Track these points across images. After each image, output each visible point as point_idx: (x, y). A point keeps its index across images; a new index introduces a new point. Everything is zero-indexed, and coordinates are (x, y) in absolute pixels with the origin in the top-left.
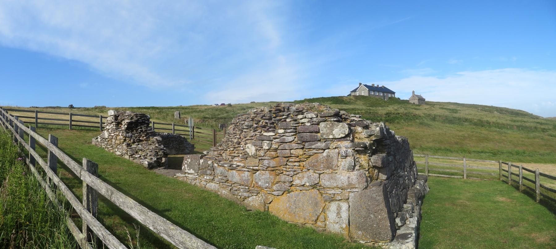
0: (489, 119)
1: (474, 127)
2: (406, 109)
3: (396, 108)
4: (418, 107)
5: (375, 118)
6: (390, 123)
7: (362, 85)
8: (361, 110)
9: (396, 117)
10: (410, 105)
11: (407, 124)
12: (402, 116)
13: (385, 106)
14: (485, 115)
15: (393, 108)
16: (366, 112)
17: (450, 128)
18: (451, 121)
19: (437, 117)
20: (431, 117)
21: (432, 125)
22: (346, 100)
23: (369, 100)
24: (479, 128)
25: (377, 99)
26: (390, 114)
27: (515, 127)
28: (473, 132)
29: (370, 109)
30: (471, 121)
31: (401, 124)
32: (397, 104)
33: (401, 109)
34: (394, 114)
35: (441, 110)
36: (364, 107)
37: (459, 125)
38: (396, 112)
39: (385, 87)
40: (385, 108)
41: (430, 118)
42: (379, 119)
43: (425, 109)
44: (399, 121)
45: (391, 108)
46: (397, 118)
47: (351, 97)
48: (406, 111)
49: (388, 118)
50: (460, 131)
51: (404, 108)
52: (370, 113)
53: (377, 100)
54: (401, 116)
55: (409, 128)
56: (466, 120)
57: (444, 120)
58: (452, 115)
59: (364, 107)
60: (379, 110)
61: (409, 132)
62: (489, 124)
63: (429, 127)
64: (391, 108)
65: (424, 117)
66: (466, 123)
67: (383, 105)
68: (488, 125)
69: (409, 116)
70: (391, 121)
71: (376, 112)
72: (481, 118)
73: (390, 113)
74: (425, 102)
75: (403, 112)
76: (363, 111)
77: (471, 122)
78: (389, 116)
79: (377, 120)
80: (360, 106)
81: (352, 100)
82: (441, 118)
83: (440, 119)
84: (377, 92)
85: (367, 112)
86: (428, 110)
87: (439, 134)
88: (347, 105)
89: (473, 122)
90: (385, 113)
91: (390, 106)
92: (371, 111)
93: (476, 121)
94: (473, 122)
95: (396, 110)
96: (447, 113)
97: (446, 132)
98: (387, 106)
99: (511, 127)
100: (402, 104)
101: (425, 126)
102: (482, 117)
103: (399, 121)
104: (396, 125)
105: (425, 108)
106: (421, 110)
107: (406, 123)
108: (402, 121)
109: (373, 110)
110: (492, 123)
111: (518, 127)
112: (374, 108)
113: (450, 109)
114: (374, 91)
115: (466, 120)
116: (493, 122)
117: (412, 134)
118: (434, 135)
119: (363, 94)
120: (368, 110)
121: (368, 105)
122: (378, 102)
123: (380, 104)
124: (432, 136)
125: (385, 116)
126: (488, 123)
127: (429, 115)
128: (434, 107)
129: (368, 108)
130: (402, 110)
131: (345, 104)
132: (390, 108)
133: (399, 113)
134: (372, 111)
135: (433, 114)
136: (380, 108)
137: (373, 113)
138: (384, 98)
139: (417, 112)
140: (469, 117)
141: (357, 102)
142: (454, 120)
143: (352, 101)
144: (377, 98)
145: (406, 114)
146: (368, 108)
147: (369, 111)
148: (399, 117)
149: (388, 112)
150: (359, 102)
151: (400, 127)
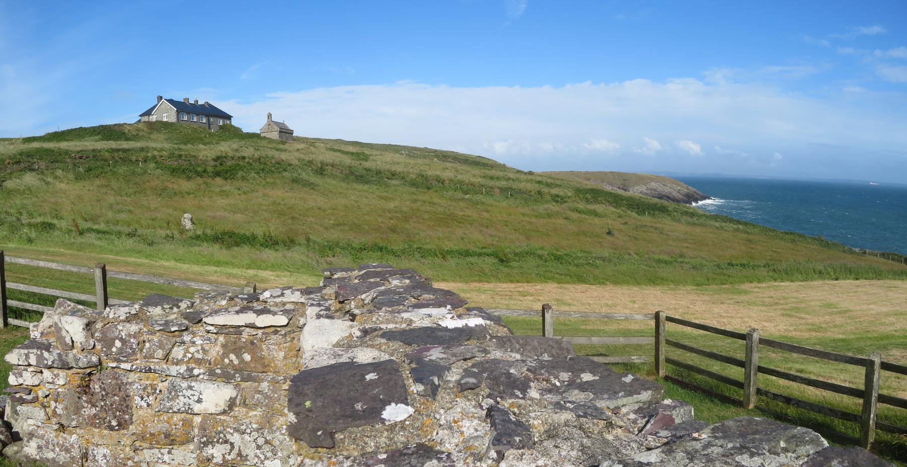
0: (438, 173)
1: (414, 189)
2: (258, 150)
3: (235, 146)
4: (281, 146)
5: (191, 168)
7: (163, 100)
8: (162, 150)
9: (239, 165)
10: (264, 143)
11: (263, 182)
12: (251, 164)
16: (171, 156)
17: (362, 193)
18: (362, 176)
22: (129, 130)
23: (178, 131)
24: (424, 192)
26: (225, 160)
27: (497, 191)
28: (416, 201)
30: (403, 178)
31: (250, 181)
33: (247, 148)
34: (233, 158)
35: (331, 153)
36: (167, 145)
38: (238, 154)
40: (212, 146)
42: (199, 169)
43: (298, 150)
45: (226, 147)
46: (241, 168)
47: (140, 126)
48: (257, 154)
49: (220, 168)
51: (252, 146)
52: (180, 156)
53: (195, 130)
54: (248, 163)
56: (393, 175)
57: (346, 175)
59: (167, 145)
62: (442, 183)
63: (313, 189)
64: (226, 147)
66: (394, 182)
67: (207, 140)
69: (265, 164)
70: (228, 175)
71: (194, 154)
72: (421, 170)
73: (225, 157)
74: (292, 137)
75: (254, 155)
76: (164, 153)
77: (404, 180)
78: (221, 164)
80: (159, 144)
81: (143, 130)
84: (194, 115)
85: (174, 154)
86: (304, 151)
89: (408, 179)
90: (213, 157)
91: (223, 143)
93: (414, 177)
94: (408, 179)
95: (237, 150)
96: (348, 160)
97: (357, 202)
98: (217, 143)
99: (490, 191)
100: (247, 140)
101: (304, 185)
102: (422, 168)
105: (296, 149)
108: (253, 174)
110: (448, 182)
111: (502, 190)
112: (189, 146)
113: (353, 154)
114: (188, 113)
115: (394, 175)
116: (451, 180)
117: (279, 204)
119: (165, 120)
120: (176, 150)
121: (175, 141)
122: (197, 135)
125: (213, 163)
127: (309, 162)
128: (314, 147)
129: (176, 146)
130: (249, 152)
131: (127, 139)
132: (223, 146)
133: (244, 158)
134: (183, 153)
136: (202, 146)
137: (186, 157)
139: (284, 156)
141: (152, 136)
142: (368, 175)
143: (141, 133)
145: (259, 159)
146: (176, 146)
147: (176, 152)
148: (245, 166)
149: (219, 154)
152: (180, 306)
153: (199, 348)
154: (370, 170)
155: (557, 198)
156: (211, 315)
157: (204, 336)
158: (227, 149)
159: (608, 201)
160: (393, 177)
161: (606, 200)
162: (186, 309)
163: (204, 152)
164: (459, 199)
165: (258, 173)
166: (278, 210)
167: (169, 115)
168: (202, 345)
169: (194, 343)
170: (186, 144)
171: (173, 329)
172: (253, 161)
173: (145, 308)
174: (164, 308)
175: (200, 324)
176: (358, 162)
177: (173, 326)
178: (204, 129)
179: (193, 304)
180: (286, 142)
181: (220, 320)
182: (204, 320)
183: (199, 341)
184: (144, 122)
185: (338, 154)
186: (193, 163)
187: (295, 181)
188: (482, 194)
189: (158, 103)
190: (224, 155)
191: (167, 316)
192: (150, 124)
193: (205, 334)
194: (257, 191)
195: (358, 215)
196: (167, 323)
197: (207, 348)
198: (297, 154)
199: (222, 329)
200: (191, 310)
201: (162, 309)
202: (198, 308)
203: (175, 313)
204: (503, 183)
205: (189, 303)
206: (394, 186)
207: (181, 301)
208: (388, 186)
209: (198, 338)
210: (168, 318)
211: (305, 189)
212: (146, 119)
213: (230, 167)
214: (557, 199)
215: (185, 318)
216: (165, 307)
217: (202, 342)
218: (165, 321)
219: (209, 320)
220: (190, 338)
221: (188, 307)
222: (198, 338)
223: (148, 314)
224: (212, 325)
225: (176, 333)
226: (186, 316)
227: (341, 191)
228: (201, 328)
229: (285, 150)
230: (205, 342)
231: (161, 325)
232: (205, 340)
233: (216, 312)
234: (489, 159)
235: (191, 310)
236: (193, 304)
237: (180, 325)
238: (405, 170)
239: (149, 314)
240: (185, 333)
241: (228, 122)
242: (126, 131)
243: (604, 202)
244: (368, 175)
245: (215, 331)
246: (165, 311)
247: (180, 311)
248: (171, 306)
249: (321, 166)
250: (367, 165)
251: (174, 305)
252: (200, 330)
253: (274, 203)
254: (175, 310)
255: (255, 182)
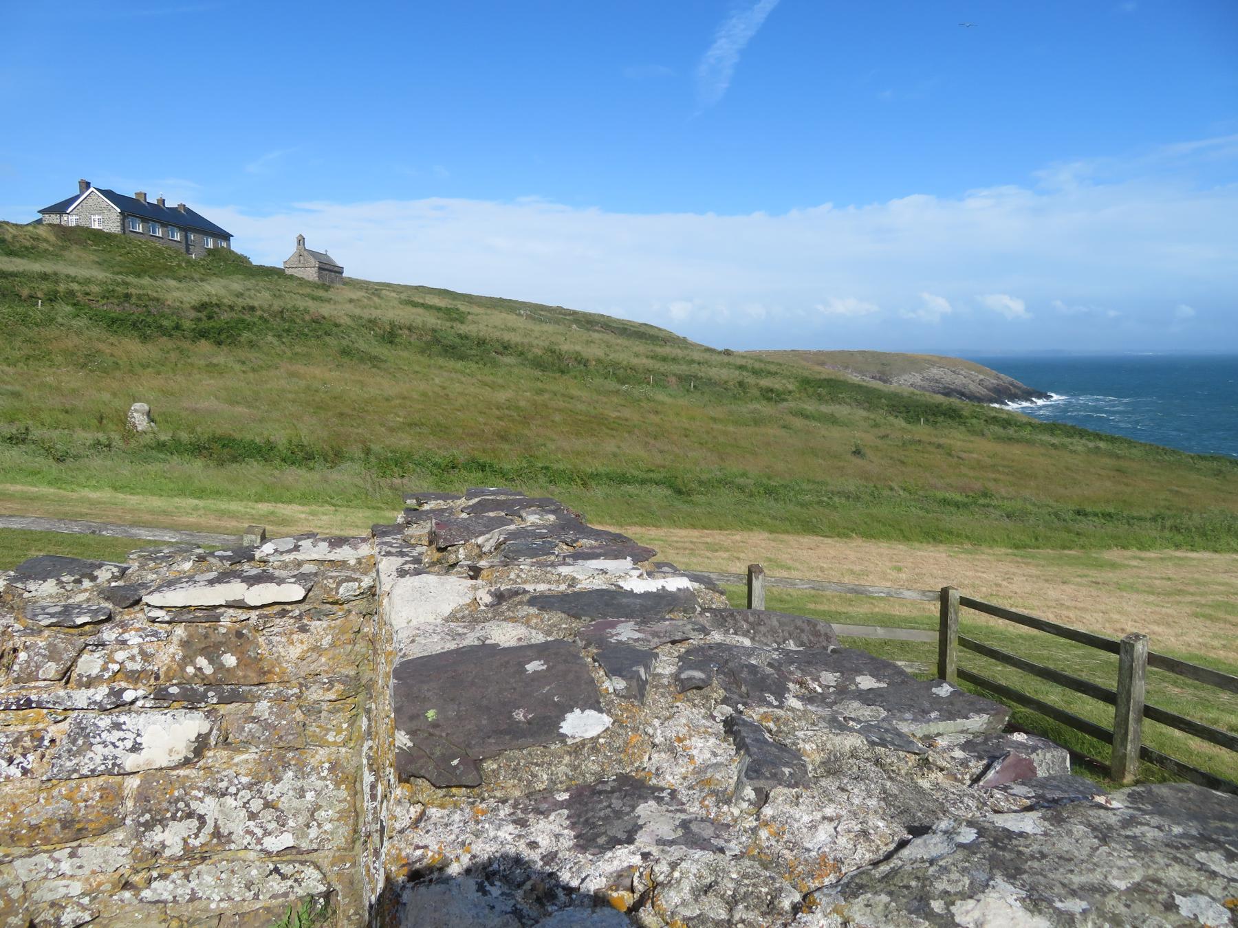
0: (578, 348)
1: (538, 373)
2: (280, 296)
4: (321, 293)
5: (149, 320)
6: (219, 343)
7: (92, 189)
8: (88, 281)
9: (243, 321)
10: (292, 285)
12: (266, 321)
13: (192, 279)
14: (562, 334)
15: (224, 287)
16: (108, 295)
17: (453, 375)
19: (400, 332)
20: (376, 329)
21: (386, 361)
22: (14, 237)
23: (124, 251)
25: (160, 251)
26: (216, 310)
27: (673, 380)
28: (540, 392)
29: (126, 284)
30: (522, 353)
32: (240, 277)
34: (231, 308)
35: (410, 309)
36: (101, 275)
37: (485, 365)
39: (189, 211)
40: (192, 284)
41: (375, 336)
42: (166, 323)
43: (351, 301)
44: (254, 338)
45: (215, 288)
46: (249, 327)
47: (42, 231)
48: (277, 305)
50: (493, 386)
51: (268, 289)
52: (127, 296)
54: (261, 318)
55: (301, 369)
56: (505, 348)
57: (427, 343)
58: (452, 327)
59: (101, 275)
60: (168, 290)
61: (303, 383)
63: (374, 366)
64: (215, 288)
65: (353, 329)
66: (507, 360)
67: (182, 273)
68: (582, 367)
69: (293, 321)
70: (223, 336)
71: (155, 294)
73: (218, 305)
74: (342, 278)
76: (95, 289)
77: (523, 357)
78: (210, 318)
79: (161, 326)
81: (46, 240)
82: (415, 336)
83: (412, 341)
85: (113, 291)
87: (424, 394)
88: (17, 260)
89: (530, 356)
90: (193, 303)
92: (132, 291)
93: (540, 353)
94: (530, 356)
96: (432, 320)
97: (444, 388)
98: (202, 280)
99: (660, 381)
101: (362, 360)
103: (254, 338)
104: (242, 353)
106: (335, 303)
107: (283, 347)
108: (270, 338)
109: (143, 288)
112: (146, 281)
113: (439, 309)
114: (145, 220)
115: (506, 348)
116: (599, 361)
118: (404, 398)
119: (96, 226)
120: (118, 284)
121: (117, 269)
123: (171, 269)
124: (398, 402)
126: (582, 361)
127: (370, 321)
128: (379, 297)
129: (119, 278)
130: (262, 297)
133: (252, 309)
135: (384, 319)
136: (172, 283)
138: (188, 250)
139: (326, 310)
140: (514, 338)
141: (66, 253)
142: (463, 345)
143: (45, 245)
144: (156, 248)
145: (282, 312)
146: (119, 278)
149: (206, 299)
150: (74, 252)
151: (260, 363)
152: (96, 577)
153: (136, 651)
154: (467, 338)
155: (770, 394)
156: (159, 589)
157: (145, 629)
158: (223, 292)
159: (856, 400)
160: (506, 352)
161: (851, 398)
162: (109, 581)
163: (177, 294)
164: (612, 392)
165: (279, 336)
166: (314, 400)
167: (106, 220)
168: (140, 645)
169: (124, 642)
170: (139, 276)
171: (79, 621)
172: (270, 315)
173: (19, 585)
174: (63, 582)
175: (137, 608)
176: (448, 324)
177: (79, 615)
178: (176, 252)
179: (123, 571)
180: (329, 287)
181: (177, 597)
182: (146, 599)
183: (134, 639)
184: (50, 225)
185: (420, 310)
186: (153, 311)
187: (346, 352)
188: (648, 383)
189: (82, 193)
190: (214, 301)
191: (68, 598)
192: (64, 233)
193: (146, 625)
194: (277, 368)
195: (446, 409)
196: (67, 611)
197: (150, 650)
198: (350, 307)
199: (180, 614)
200: (121, 583)
201: (57, 584)
202: (134, 578)
203: (85, 590)
204: (683, 369)
205: (115, 570)
206: (511, 366)
207: (100, 566)
208: (495, 364)
209: (133, 633)
210: (71, 601)
211: (362, 366)
212: (54, 219)
213: (227, 323)
214: (768, 395)
215: (107, 599)
216: (64, 579)
217: (140, 640)
218: (64, 606)
219: (154, 599)
220: (115, 635)
221: (115, 578)
222: (133, 633)
223: (26, 595)
224: (161, 608)
225: (87, 628)
226: (109, 594)
227: (417, 368)
228: (140, 615)
229: (329, 301)
230: (148, 639)
231: (52, 615)
232: (147, 636)
233: (170, 584)
234: (660, 329)
235: (121, 583)
236: (123, 571)
237: (96, 612)
238: (526, 340)
239: (30, 595)
240: (105, 627)
241: (224, 244)
242: (8, 237)
243: (848, 400)
244: (463, 345)
245: (167, 618)
246: (63, 587)
247: (97, 586)
248: (77, 577)
249: (392, 329)
250: (463, 329)
251: (83, 576)
252: (138, 618)
253: (308, 388)
254: (87, 584)
255: (273, 351)
